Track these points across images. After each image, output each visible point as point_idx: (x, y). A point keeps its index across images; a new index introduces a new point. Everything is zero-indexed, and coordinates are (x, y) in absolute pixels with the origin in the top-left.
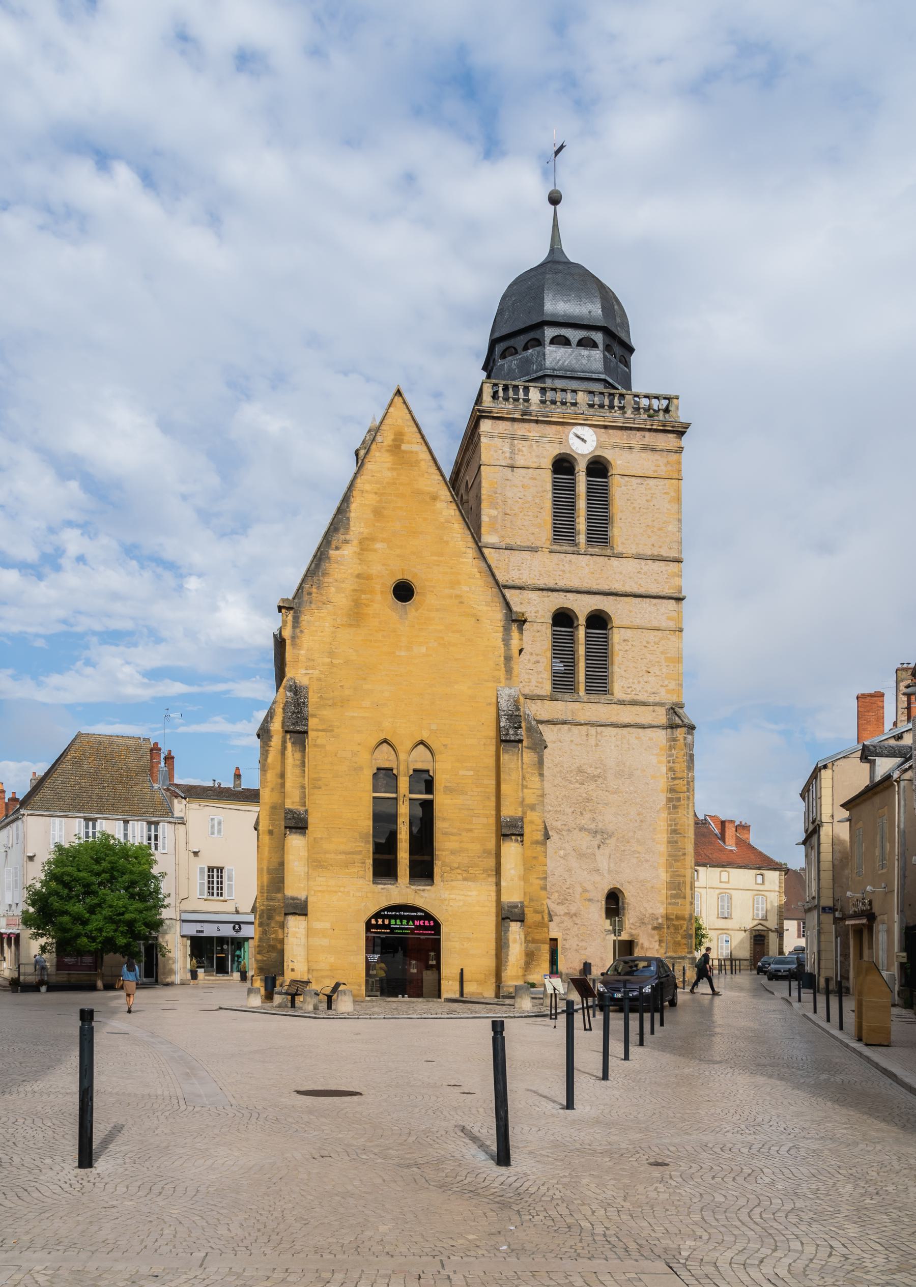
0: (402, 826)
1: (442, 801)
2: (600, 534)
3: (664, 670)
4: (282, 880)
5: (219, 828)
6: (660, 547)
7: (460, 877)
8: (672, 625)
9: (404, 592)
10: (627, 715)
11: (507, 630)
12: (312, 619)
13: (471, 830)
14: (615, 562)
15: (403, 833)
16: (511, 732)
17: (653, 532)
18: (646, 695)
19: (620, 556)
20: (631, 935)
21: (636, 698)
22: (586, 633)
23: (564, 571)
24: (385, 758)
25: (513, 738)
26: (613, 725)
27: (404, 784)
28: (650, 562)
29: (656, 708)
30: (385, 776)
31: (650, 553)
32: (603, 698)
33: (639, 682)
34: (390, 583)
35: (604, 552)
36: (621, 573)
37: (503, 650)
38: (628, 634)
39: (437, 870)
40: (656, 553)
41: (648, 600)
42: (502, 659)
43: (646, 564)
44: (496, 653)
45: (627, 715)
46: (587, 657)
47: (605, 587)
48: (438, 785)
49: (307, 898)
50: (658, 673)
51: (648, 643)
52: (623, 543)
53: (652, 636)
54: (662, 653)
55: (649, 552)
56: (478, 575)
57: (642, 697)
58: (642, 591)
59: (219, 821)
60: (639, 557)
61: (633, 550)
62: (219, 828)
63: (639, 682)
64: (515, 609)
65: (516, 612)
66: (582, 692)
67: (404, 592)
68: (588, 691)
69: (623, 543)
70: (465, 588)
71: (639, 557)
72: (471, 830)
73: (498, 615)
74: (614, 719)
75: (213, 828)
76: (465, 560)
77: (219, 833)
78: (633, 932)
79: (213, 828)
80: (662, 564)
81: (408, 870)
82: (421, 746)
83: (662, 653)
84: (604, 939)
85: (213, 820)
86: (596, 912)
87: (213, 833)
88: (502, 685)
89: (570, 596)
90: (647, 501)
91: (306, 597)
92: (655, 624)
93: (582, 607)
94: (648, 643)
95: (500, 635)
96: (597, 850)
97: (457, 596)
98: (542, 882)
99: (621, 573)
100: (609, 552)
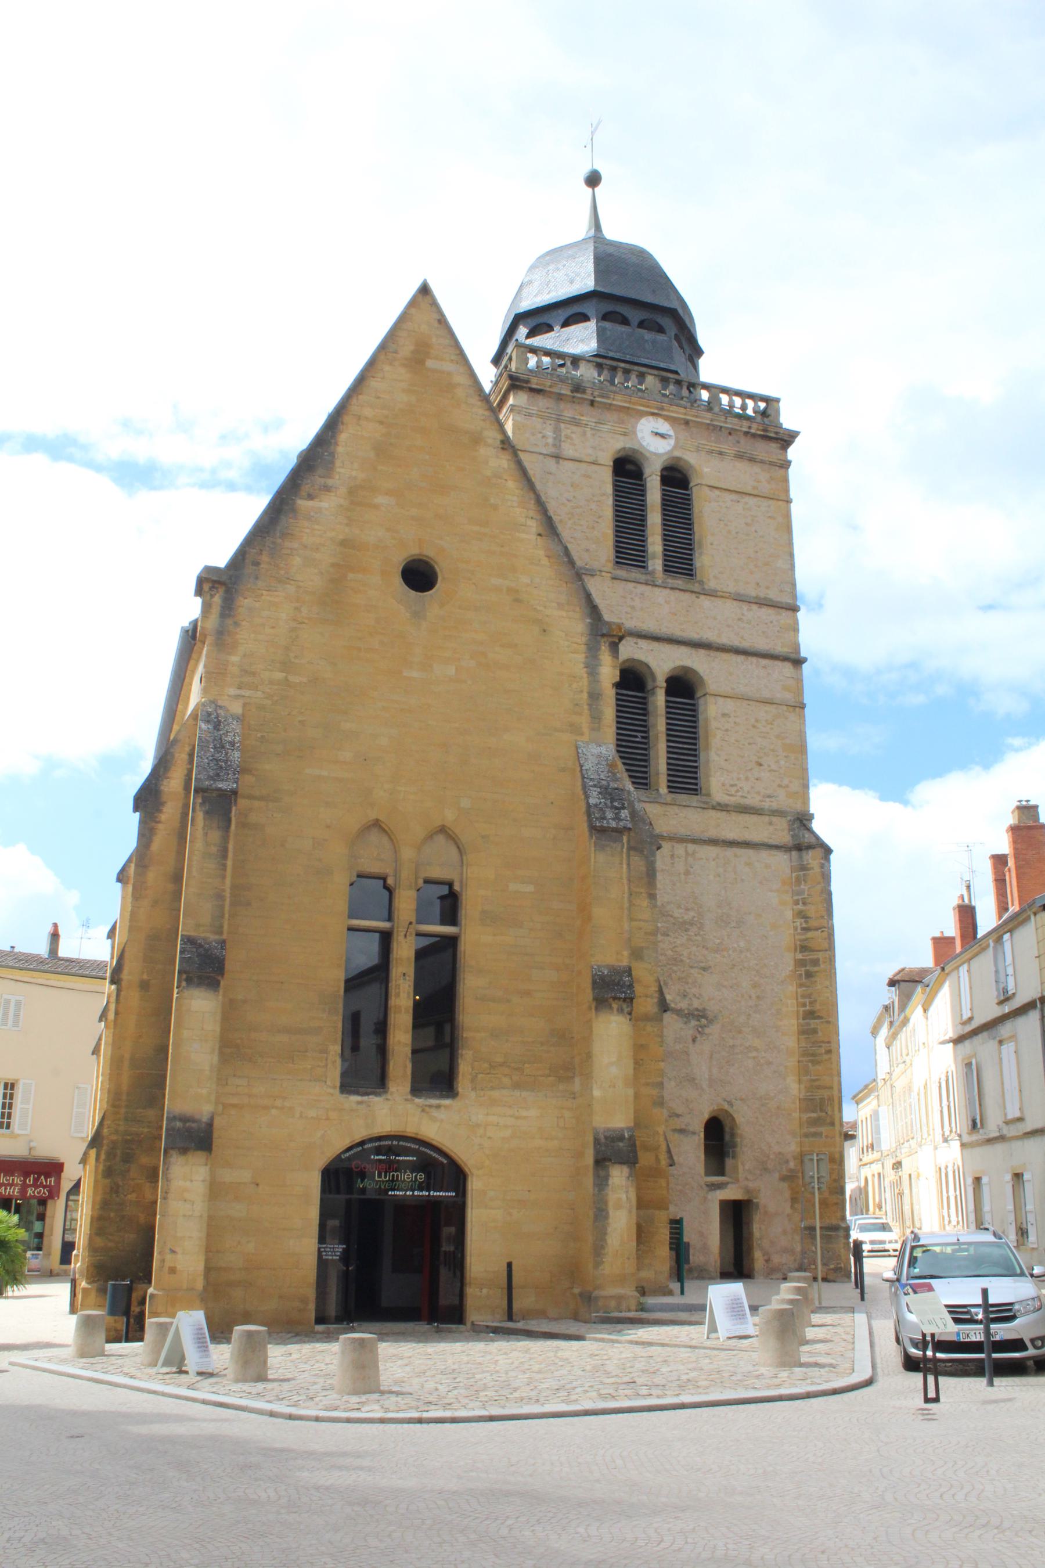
0: (401, 981)
1: (475, 939)
2: (681, 561)
3: (782, 762)
4: (160, 1083)
5: (17, 1015)
6: (767, 588)
7: (506, 1081)
8: (788, 696)
9: (419, 576)
10: (732, 827)
11: (592, 651)
12: (257, 605)
13: (528, 993)
14: (705, 602)
15: (403, 995)
16: (609, 814)
17: (756, 566)
18: (758, 798)
19: (712, 594)
20: (748, 1191)
21: (743, 801)
22: (667, 701)
23: (633, 607)
24: (374, 858)
25: (613, 824)
26: (713, 842)
27: (406, 904)
28: (754, 607)
29: (774, 819)
30: (375, 890)
31: (754, 594)
32: (694, 800)
33: (747, 779)
34: (398, 560)
35: (690, 587)
36: (715, 619)
37: (585, 682)
38: (729, 705)
39: (464, 1068)
40: (762, 595)
41: (754, 660)
42: (585, 696)
43: (749, 610)
44: (574, 686)
45: (732, 827)
46: (670, 737)
47: (693, 635)
48: (470, 908)
49: (212, 1119)
50: (774, 767)
51: (757, 721)
52: (715, 577)
53: (764, 713)
54: (778, 737)
55: (752, 592)
56: (545, 561)
57: (753, 800)
58: (745, 645)
59: (18, 1004)
60: (739, 598)
61: (731, 588)
62: (17, 1015)
63: (747, 779)
64: (607, 617)
65: (608, 623)
66: (663, 790)
67: (419, 576)
68: (672, 788)
69: (715, 577)
70: (525, 580)
71: (739, 598)
72: (528, 993)
73: (578, 626)
74: (713, 833)
75: (5, 1015)
76: (523, 536)
77: (16, 1023)
78: (751, 1185)
79: (5, 1015)
80: (770, 611)
81: (409, 1066)
82: (441, 839)
83: (778, 737)
84: (705, 1198)
85: (8, 1002)
86: (691, 1152)
87: (5, 1023)
88: (586, 738)
89: (643, 644)
90: (746, 524)
91: (249, 569)
92: (766, 694)
93: (661, 662)
94: (757, 721)
95: (581, 657)
96: (691, 1046)
97: (510, 590)
98: (655, 1092)
99: (715, 619)
100: (696, 587)
